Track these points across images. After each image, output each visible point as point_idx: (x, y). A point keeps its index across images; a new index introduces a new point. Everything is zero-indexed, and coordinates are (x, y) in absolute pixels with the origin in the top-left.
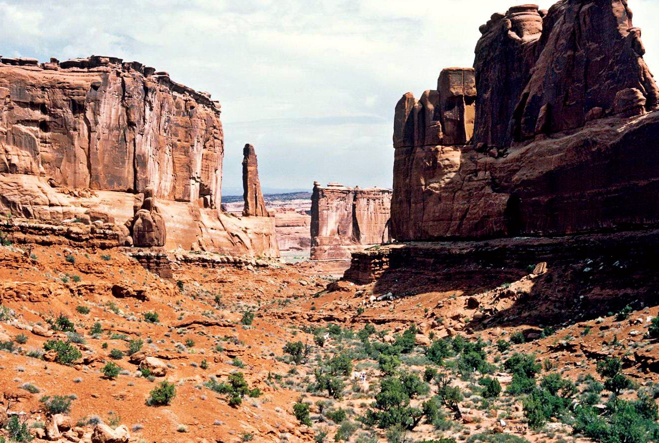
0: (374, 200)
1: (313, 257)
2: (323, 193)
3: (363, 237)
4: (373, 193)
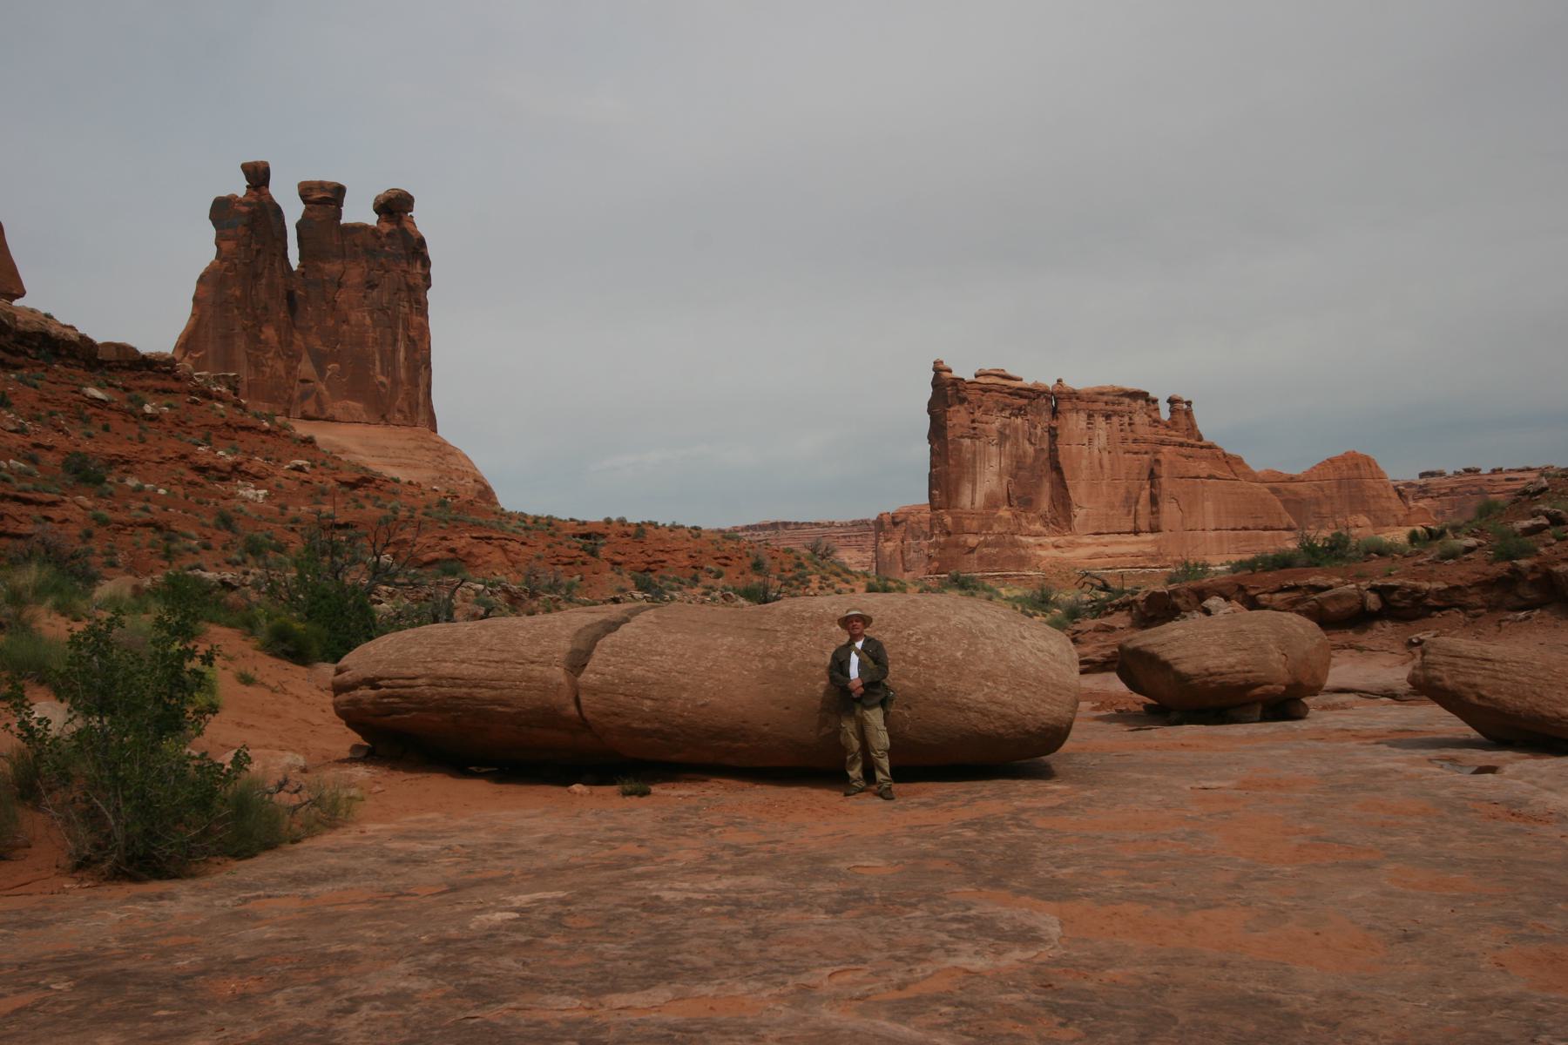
0: (1108, 417)
3: (1079, 514)
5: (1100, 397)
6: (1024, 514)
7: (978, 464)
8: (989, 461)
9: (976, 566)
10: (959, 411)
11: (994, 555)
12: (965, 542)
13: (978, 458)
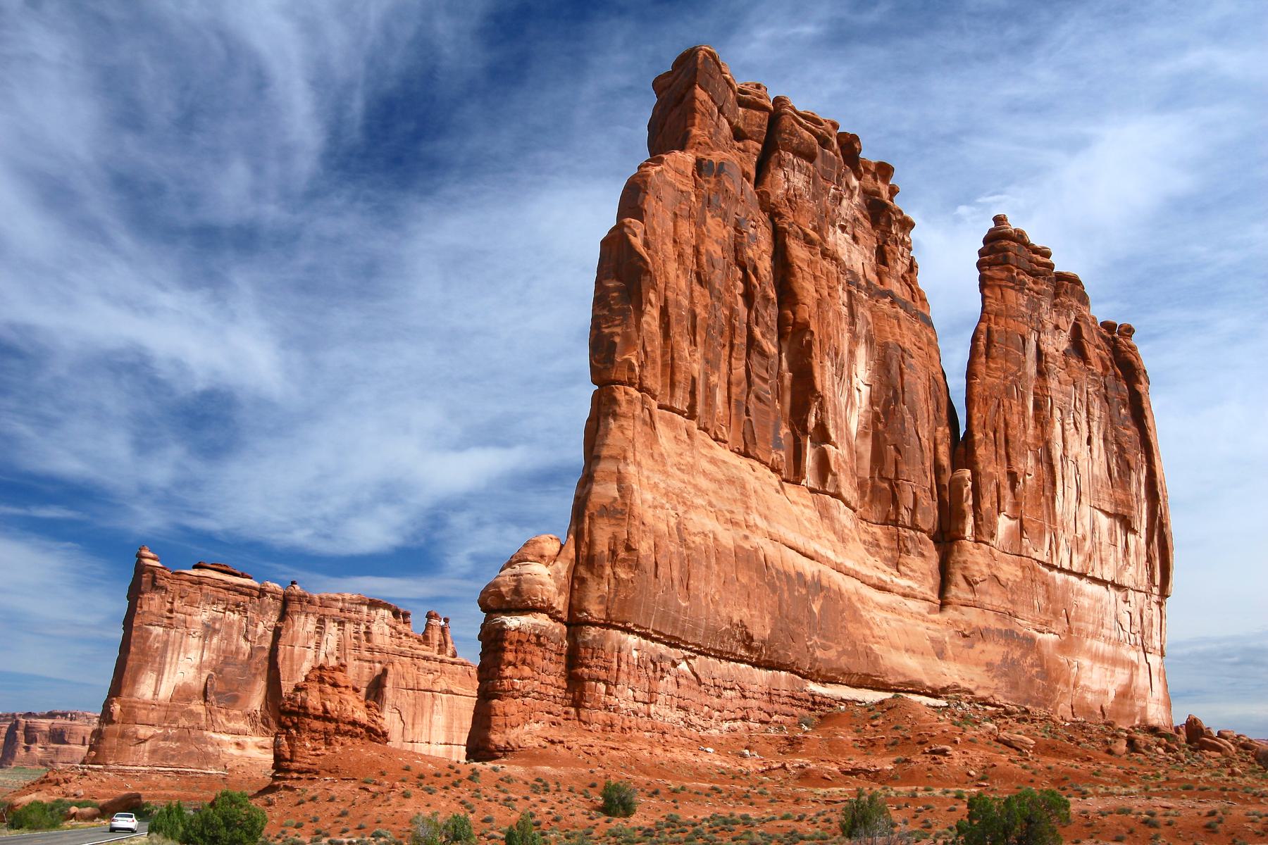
0: (341, 623)
1: (93, 753)
2: (154, 579)
4: (340, 605)
5: (334, 603)
6: (224, 711)
7: (169, 655)
8: (186, 652)
9: (146, 759)
10: (152, 599)
11: (174, 750)
12: (135, 733)
13: (170, 648)
